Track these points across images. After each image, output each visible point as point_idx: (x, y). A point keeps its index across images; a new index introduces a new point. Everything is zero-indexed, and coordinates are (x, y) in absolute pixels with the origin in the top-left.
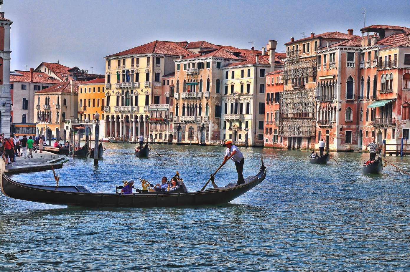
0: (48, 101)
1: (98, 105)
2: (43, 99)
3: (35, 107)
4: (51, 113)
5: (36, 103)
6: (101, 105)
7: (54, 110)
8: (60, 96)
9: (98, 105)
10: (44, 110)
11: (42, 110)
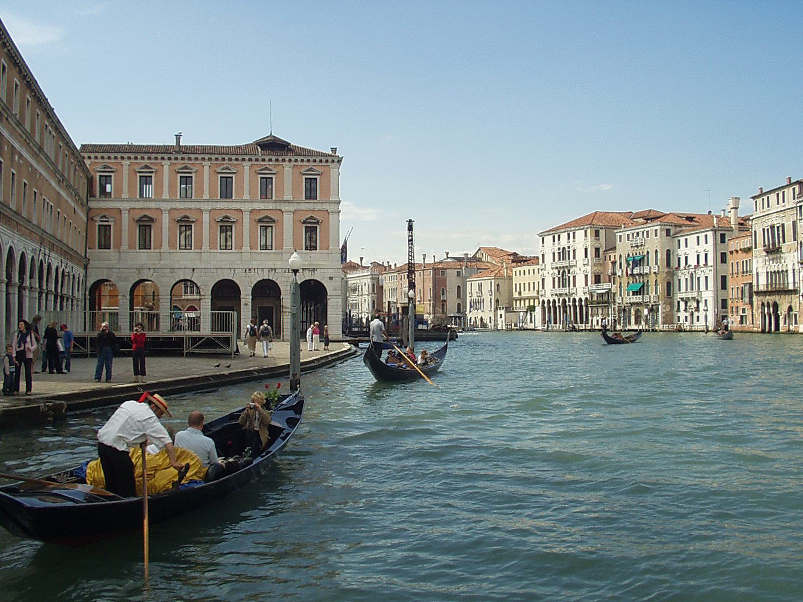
0: (480, 286)
1: (534, 289)
2: (475, 285)
3: (468, 294)
4: (483, 300)
5: (468, 290)
6: (536, 289)
7: (486, 297)
8: (493, 281)
9: (534, 289)
10: (477, 298)
11: (475, 297)
